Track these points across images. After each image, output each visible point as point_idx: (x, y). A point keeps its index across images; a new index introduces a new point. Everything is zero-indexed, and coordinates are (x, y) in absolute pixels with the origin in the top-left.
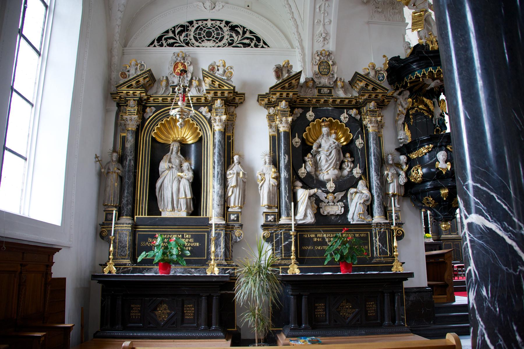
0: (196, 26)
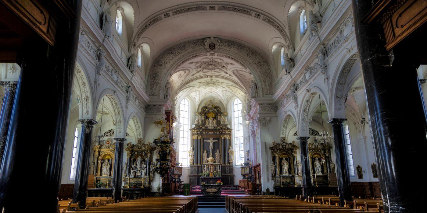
0: (113, 131)
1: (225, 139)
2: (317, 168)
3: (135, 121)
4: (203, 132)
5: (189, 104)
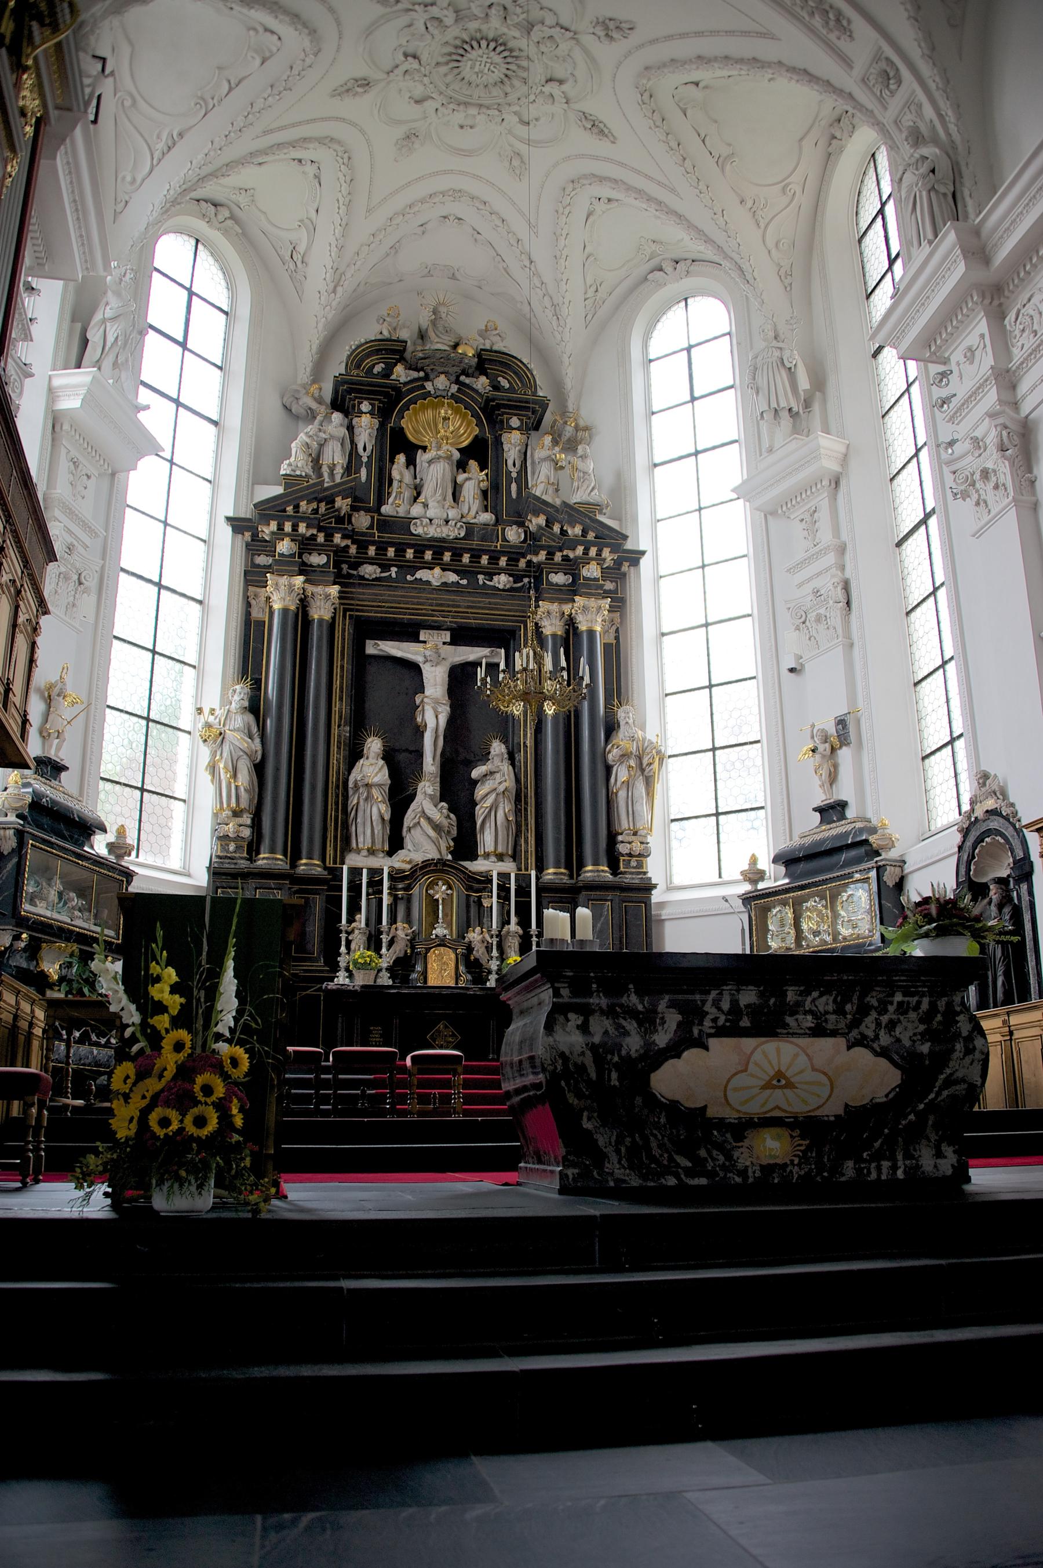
4: (355, 566)
5: (233, 299)
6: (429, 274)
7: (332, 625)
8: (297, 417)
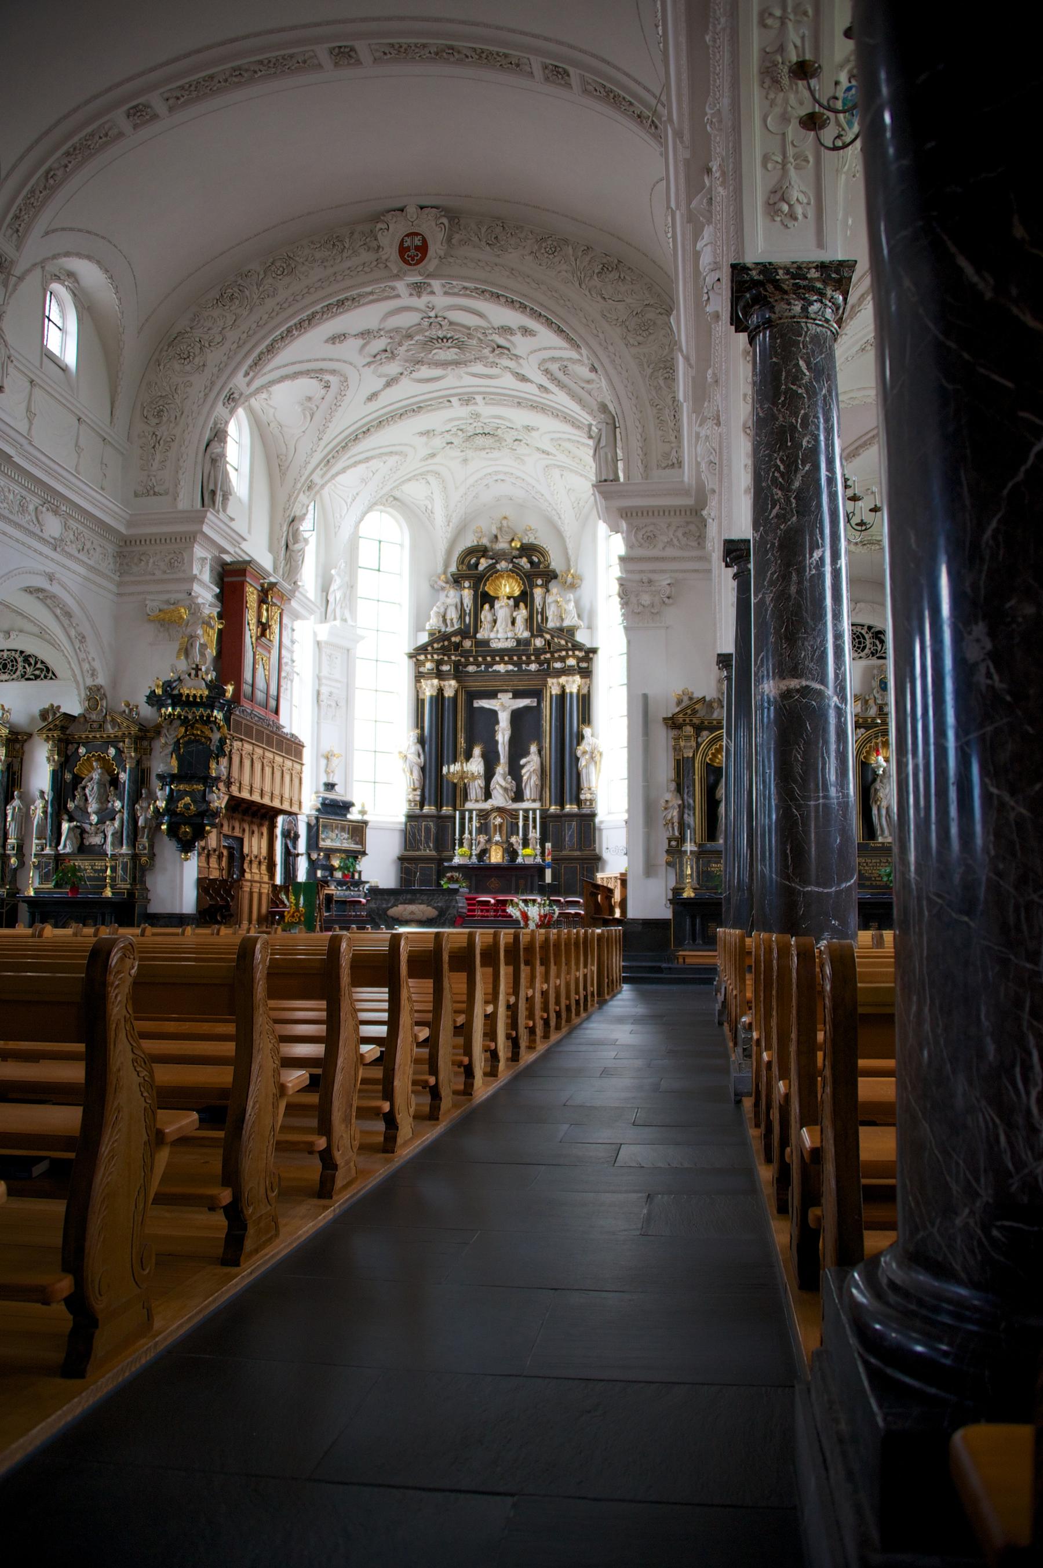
1: (562, 696)
2: (884, 812)
3: (58, 611)
4: (466, 666)
6: (498, 500)
7: (455, 697)
8: (437, 591)
